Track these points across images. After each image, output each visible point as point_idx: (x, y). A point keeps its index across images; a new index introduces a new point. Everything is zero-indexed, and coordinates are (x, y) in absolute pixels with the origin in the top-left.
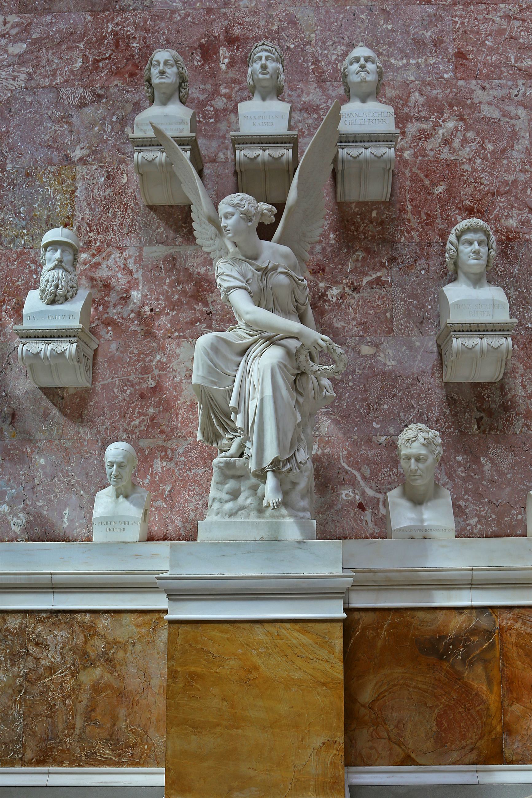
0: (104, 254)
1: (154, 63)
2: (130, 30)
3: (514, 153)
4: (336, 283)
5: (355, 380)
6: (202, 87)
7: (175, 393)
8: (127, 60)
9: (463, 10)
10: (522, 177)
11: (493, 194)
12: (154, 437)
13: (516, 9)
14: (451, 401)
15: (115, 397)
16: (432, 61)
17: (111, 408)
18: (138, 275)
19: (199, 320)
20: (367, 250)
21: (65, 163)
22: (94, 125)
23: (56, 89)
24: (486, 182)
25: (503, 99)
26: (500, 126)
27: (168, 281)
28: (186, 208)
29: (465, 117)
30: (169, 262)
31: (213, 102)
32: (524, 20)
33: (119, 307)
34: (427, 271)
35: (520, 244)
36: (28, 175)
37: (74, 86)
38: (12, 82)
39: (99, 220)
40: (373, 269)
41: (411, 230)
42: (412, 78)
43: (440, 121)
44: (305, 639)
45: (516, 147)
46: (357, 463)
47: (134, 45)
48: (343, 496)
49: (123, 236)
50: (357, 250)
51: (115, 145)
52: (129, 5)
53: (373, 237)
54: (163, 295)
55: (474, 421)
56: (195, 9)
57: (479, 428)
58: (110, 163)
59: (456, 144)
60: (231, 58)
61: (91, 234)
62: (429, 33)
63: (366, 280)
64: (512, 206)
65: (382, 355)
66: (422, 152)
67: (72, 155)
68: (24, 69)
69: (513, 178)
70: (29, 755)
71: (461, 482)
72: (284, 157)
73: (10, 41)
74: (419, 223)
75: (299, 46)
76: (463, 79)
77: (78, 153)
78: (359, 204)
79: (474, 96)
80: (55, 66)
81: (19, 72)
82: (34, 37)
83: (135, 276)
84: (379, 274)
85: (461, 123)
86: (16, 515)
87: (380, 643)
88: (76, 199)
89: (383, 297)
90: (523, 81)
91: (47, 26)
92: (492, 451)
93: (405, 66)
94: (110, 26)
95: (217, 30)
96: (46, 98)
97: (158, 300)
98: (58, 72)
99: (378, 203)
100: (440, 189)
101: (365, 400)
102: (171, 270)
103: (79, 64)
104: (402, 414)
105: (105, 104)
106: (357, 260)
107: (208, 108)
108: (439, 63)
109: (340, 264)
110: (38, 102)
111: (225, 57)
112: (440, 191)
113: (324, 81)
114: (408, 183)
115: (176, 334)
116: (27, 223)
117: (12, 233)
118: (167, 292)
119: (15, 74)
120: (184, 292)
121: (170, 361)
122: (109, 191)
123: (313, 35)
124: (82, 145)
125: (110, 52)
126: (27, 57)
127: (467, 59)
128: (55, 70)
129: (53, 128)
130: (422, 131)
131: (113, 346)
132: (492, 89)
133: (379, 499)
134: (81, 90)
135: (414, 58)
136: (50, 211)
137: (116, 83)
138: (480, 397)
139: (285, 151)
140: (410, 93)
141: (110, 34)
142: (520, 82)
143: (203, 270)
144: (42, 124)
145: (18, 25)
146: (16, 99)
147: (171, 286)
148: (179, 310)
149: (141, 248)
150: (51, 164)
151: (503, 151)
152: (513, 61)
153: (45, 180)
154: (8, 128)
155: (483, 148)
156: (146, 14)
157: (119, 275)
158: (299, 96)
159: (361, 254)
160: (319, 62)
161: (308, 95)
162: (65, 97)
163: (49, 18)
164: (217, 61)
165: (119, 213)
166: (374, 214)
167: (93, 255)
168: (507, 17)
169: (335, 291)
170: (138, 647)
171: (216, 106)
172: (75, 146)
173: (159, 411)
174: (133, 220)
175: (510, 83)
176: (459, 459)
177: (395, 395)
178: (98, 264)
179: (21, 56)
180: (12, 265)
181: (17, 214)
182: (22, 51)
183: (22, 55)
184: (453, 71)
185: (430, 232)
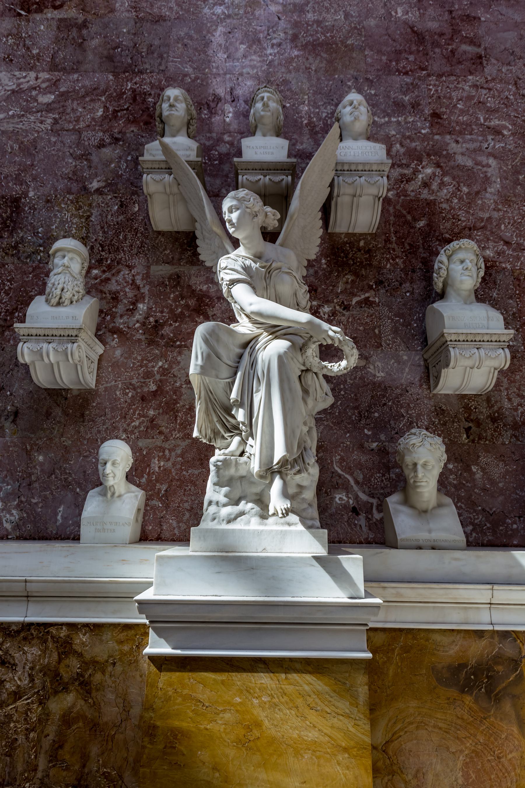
0: (114, 271)
1: (165, 98)
2: (147, 88)
3: (488, 195)
4: (328, 302)
5: (346, 389)
7: (174, 397)
8: (143, 111)
9: (437, 80)
10: (496, 215)
11: (470, 229)
12: (153, 438)
13: (483, 80)
15: (117, 399)
16: (410, 119)
17: (113, 409)
20: (356, 274)
21: (83, 193)
22: (111, 162)
23: (79, 132)
24: (463, 219)
25: (475, 150)
26: (474, 173)
27: (172, 296)
28: (191, 234)
29: (442, 164)
30: (174, 280)
31: (218, 148)
32: (490, 89)
33: (125, 317)
34: (412, 293)
35: (497, 272)
36: (48, 201)
37: (95, 130)
38: (39, 125)
39: (112, 241)
40: (362, 290)
41: (396, 257)
42: (393, 133)
43: (420, 168)
45: (489, 190)
47: (150, 100)
48: (337, 500)
49: (132, 256)
50: (346, 274)
51: (129, 180)
52: (147, 69)
53: (361, 262)
54: (167, 308)
55: (462, 430)
56: (204, 74)
57: (468, 437)
58: (123, 194)
61: (103, 253)
62: (407, 98)
63: (355, 300)
64: (488, 239)
65: (372, 367)
67: (90, 186)
68: (51, 115)
69: (487, 215)
71: (453, 490)
72: (284, 182)
73: (40, 92)
74: (403, 252)
75: (294, 105)
76: (439, 134)
77: (95, 185)
78: (348, 235)
79: (449, 148)
80: (78, 114)
81: (46, 117)
82: (61, 90)
83: (142, 291)
84: (367, 295)
85: (438, 170)
88: (91, 224)
89: (372, 316)
90: (493, 137)
91: (74, 82)
92: (483, 460)
93: (387, 123)
94: (129, 85)
97: (162, 312)
98: (81, 119)
99: (365, 234)
100: (422, 224)
101: (356, 408)
102: (175, 286)
103: (100, 113)
104: (392, 422)
105: (122, 146)
106: (347, 283)
107: (213, 152)
108: (417, 121)
109: (331, 285)
110: (62, 142)
111: (229, 112)
112: (421, 225)
113: (316, 133)
114: (392, 218)
115: (178, 343)
116: (44, 242)
117: (30, 250)
118: (171, 305)
119: (43, 119)
120: (187, 306)
121: (171, 367)
122: (121, 218)
123: (306, 97)
124: (99, 179)
125: (128, 105)
126: (55, 105)
127: (441, 119)
129: (74, 163)
130: (403, 175)
131: (118, 352)
132: (465, 142)
134: (101, 134)
135: (394, 117)
136: (66, 232)
137: (132, 129)
139: (285, 177)
140: (392, 145)
141: (129, 90)
142: (490, 137)
143: (205, 288)
144: (63, 160)
145: (48, 80)
146: (42, 139)
147: (175, 300)
148: (181, 322)
149: (149, 267)
150: (70, 192)
151: (477, 193)
152: (482, 121)
153: (63, 206)
155: (459, 190)
156: (161, 76)
157: (127, 290)
159: (350, 278)
161: (302, 144)
162: (85, 139)
163: (76, 76)
165: (129, 236)
166: (362, 243)
167: (104, 272)
168: (475, 86)
171: (221, 151)
172: (93, 179)
173: (159, 414)
174: (142, 242)
175: (480, 138)
177: (385, 404)
178: (108, 280)
179: (49, 104)
180: (27, 277)
181: (36, 234)
182: (50, 101)
184: (429, 128)
185: (414, 260)
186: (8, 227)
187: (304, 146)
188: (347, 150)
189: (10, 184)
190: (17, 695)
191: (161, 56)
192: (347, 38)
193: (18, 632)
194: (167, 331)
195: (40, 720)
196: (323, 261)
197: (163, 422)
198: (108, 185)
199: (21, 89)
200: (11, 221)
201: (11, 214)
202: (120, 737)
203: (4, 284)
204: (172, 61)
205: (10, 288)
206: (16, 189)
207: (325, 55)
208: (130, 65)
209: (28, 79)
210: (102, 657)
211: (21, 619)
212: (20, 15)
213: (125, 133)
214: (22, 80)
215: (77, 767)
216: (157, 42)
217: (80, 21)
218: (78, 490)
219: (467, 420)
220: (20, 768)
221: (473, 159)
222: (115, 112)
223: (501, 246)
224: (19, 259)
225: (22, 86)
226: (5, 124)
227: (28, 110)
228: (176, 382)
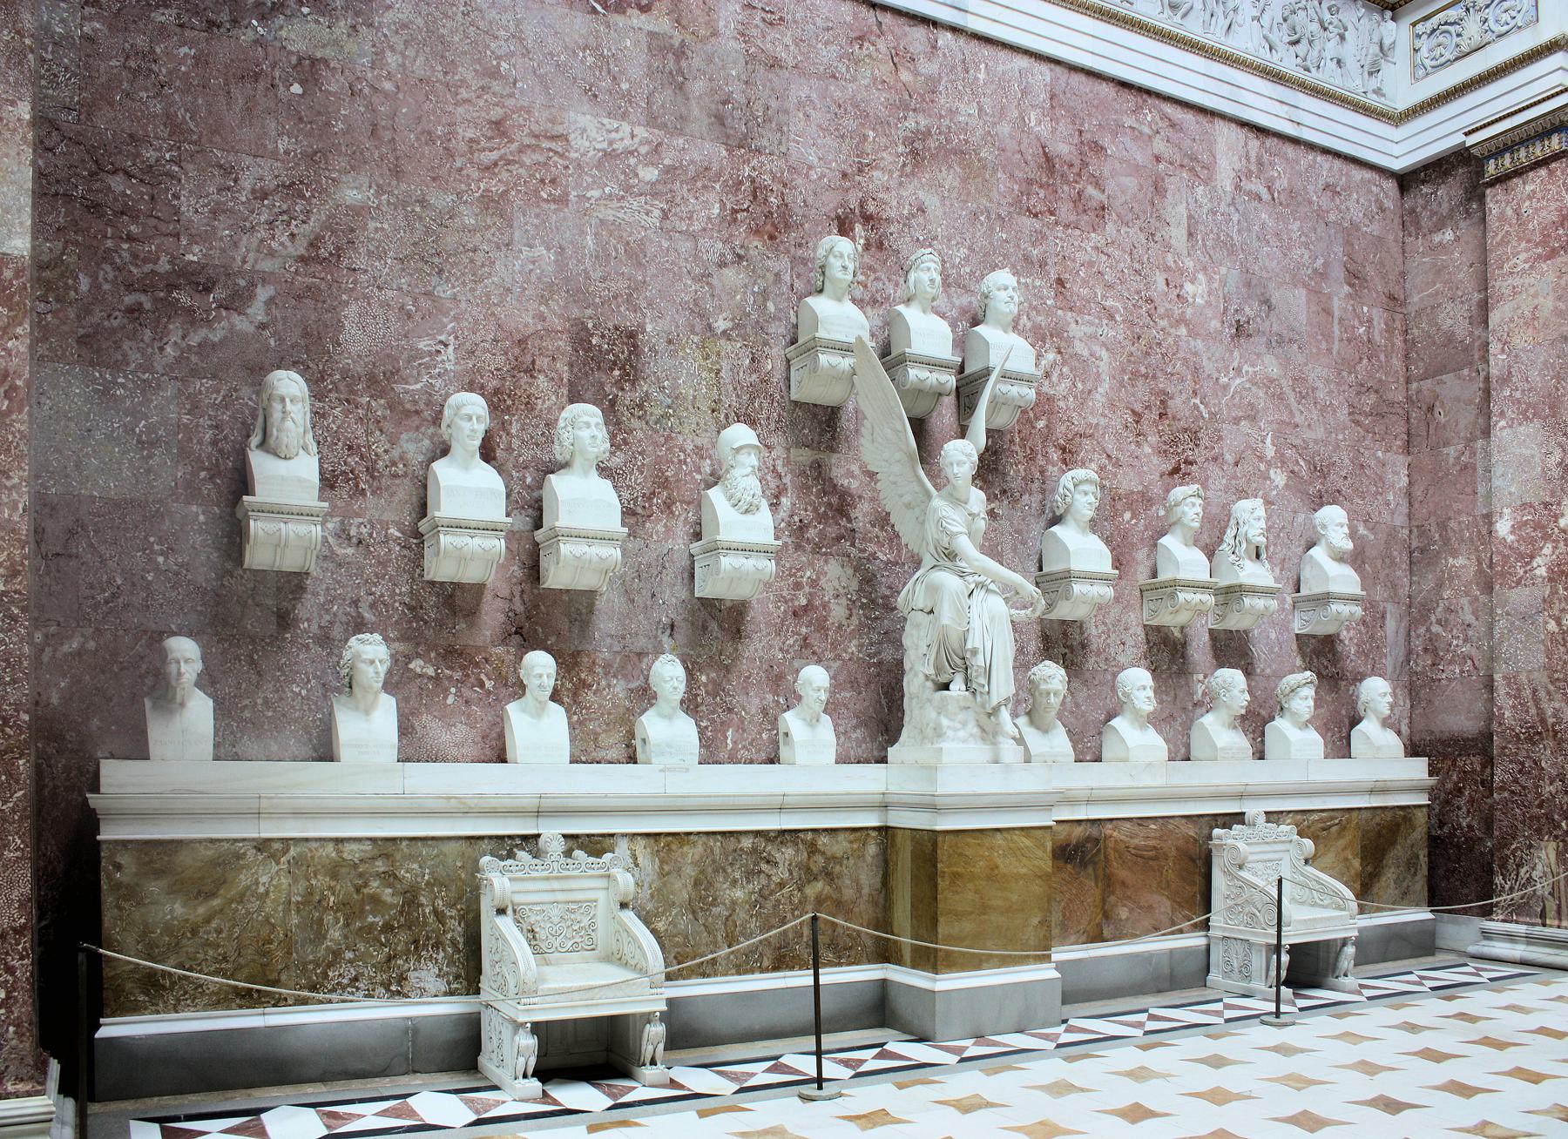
8: (766, 217)
21: (708, 334)
23: (694, 237)
36: (670, 342)
47: (772, 199)
51: (758, 322)
70: (766, 963)
77: (721, 325)
82: (667, 162)
96: (685, 246)
103: (716, 211)
105: (746, 268)
111: (861, 237)
117: (658, 412)
120: (830, 505)
124: (724, 315)
126: (660, 187)
134: (720, 245)
137: (755, 243)
141: (747, 178)
145: (648, 142)
154: (644, 277)
156: (781, 162)
163: (681, 141)
174: (779, 415)
183: (653, 184)
189: (622, 309)
190: (782, 885)
191: (780, 130)
193: (776, 837)
194: (812, 533)
195: (800, 902)
197: (815, 640)
198: (737, 326)
199: (614, 150)
200: (631, 366)
201: (630, 355)
202: (855, 910)
204: (794, 141)
206: (629, 320)
208: (745, 136)
209: (620, 135)
211: (779, 827)
212: (594, 10)
213: (747, 249)
214: (614, 135)
216: (774, 104)
217: (676, 42)
219: (1065, 646)
224: (647, 423)
226: (602, 208)
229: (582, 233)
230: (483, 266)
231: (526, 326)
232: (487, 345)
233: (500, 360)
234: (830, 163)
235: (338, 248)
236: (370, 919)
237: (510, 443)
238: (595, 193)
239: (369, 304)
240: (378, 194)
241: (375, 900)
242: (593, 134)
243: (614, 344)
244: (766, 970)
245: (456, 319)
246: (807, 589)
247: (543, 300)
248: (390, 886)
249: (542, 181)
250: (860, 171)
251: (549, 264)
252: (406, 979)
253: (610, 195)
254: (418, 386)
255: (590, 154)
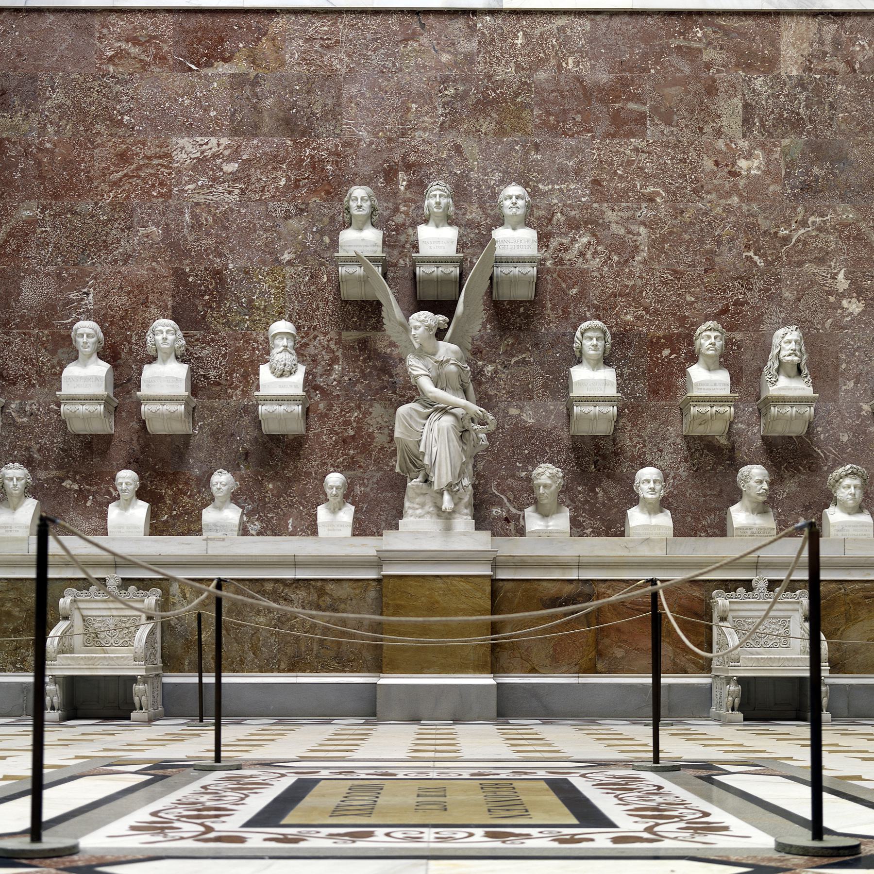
3: (635, 263)
4: (491, 362)
6: (385, 205)
7: (369, 440)
9: (600, 143)
10: (640, 282)
12: (354, 470)
13: (644, 143)
14: (575, 449)
16: (572, 186)
17: (321, 450)
18: (339, 354)
19: (386, 388)
20: (517, 338)
24: (611, 286)
25: (628, 219)
27: (361, 358)
29: (597, 233)
31: (394, 218)
32: (650, 153)
37: (280, 200)
40: (520, 352)
42: (556, 201)
43: (577, 237)
44: (468, 586)
45: (637, 258)
46: (504, 490)
47: (328, 167)
48: (494, 512)
50: (507, 338)
51: (316, 251)
52: (323, 133)
54: (358, 368)
56: (378, 138)
58: (312, 265)
59: (589, 256)
60: (409, 181)
61: (300, 321)
62: (571, 163)
63: (514, 360)
66: (560, 262)
68: (237, 185)
69: (632, 283)
74: (556, 318)
75: (464, 172)
77: (286, 257)
79: (605, 216)
80: (263, 184)
81: (233, 187)
84: (524, 356)
86: (253, 523)
87: (516, 601)
89: (527, 373)
91: (254, 148)
93: (550, 190)
94: (308, 151)
95: (397, 158)
97: (354, 372)
99: (526, 302)
100: (574, 291)
103: (283, 183)
106: (508, 345)
108: (579, 189)
109: (494, 348)
111: (404, 180)
112: (574, 292)
115: (369, 397)
118: (361, 366)
119: (230, 189)
124: (289, 250)
127: (601, 186)
128: (264, 187)
129: (265, 235)
131: (321, 406)
132: (620, 211)
133: (520, 515)
134: (286, 205)
135: (558, 184)
136: (266, 302)
137: (314, 199)
138: (597, 446)
140: (553, 214)
141: (307, 157)
142: (644, 205)
144: (255, 232)
147: (364, 361)
151: (626, 261)
152: (639, 187)
153: (261, 277)
155: (610, 259)
157: (324, 353)
158: (464, 214)
160: (481, 186)
161: (471, 213)
162: (273, 210)
163: (255, 141)
164: (397, 183)
165: (321, 305)
166: (522, 310)
169: (490, 368)
170: (354, 602)
171: (397, 221)
173: (357, 453)
176: (580, 488)
178: (306, 345)
180: (239, 343)
186: (215, 298)
187: (474, 215)
188: (505, 244)
189: (211, 257)
192: (517, 95)
196: (488, 326)
197: (361, 459)
199: (205, 156)
200: (218, 292)
203: (220, 349)
204: (347, 124)
205: (226, 353)
206: (218, 262)
207: (494, 116)
209: (210, 146)
210: (344, 597)
212: (190, 69)
214: (205, 147)
215: (335, 649)
217: (252, 77)
218: (301, 508)
220: (303, 649)
221: (626, 228)
222: (297, 180)
223: (641, 312)
225: (205, 154)
226: (196, 195)
227: (215, 179)
228: (369, 428)
229: (182, 213)
230: (112, 243)
231: (142, 275)
232: (115, 291)
233: (124, 299)
234: (378, 133)
235: (17, 247)
236: (5, 625)
237: (130, 349)
238: (191, 187)
239: (38, 276)
240: (42, 212)
241: (9, 614)
242: (189, 148)
243: (205, 280)
244: (283, 671)
245: (95, 278)
246: (355, 425)
247: (154, 258)
248: (18, 606)
249: (153, 185)
250: (403, 135)
251: (159, 236)
252: (26, 661)
253: (202, 185)
254: (70, 320)
255: (187, 163)
